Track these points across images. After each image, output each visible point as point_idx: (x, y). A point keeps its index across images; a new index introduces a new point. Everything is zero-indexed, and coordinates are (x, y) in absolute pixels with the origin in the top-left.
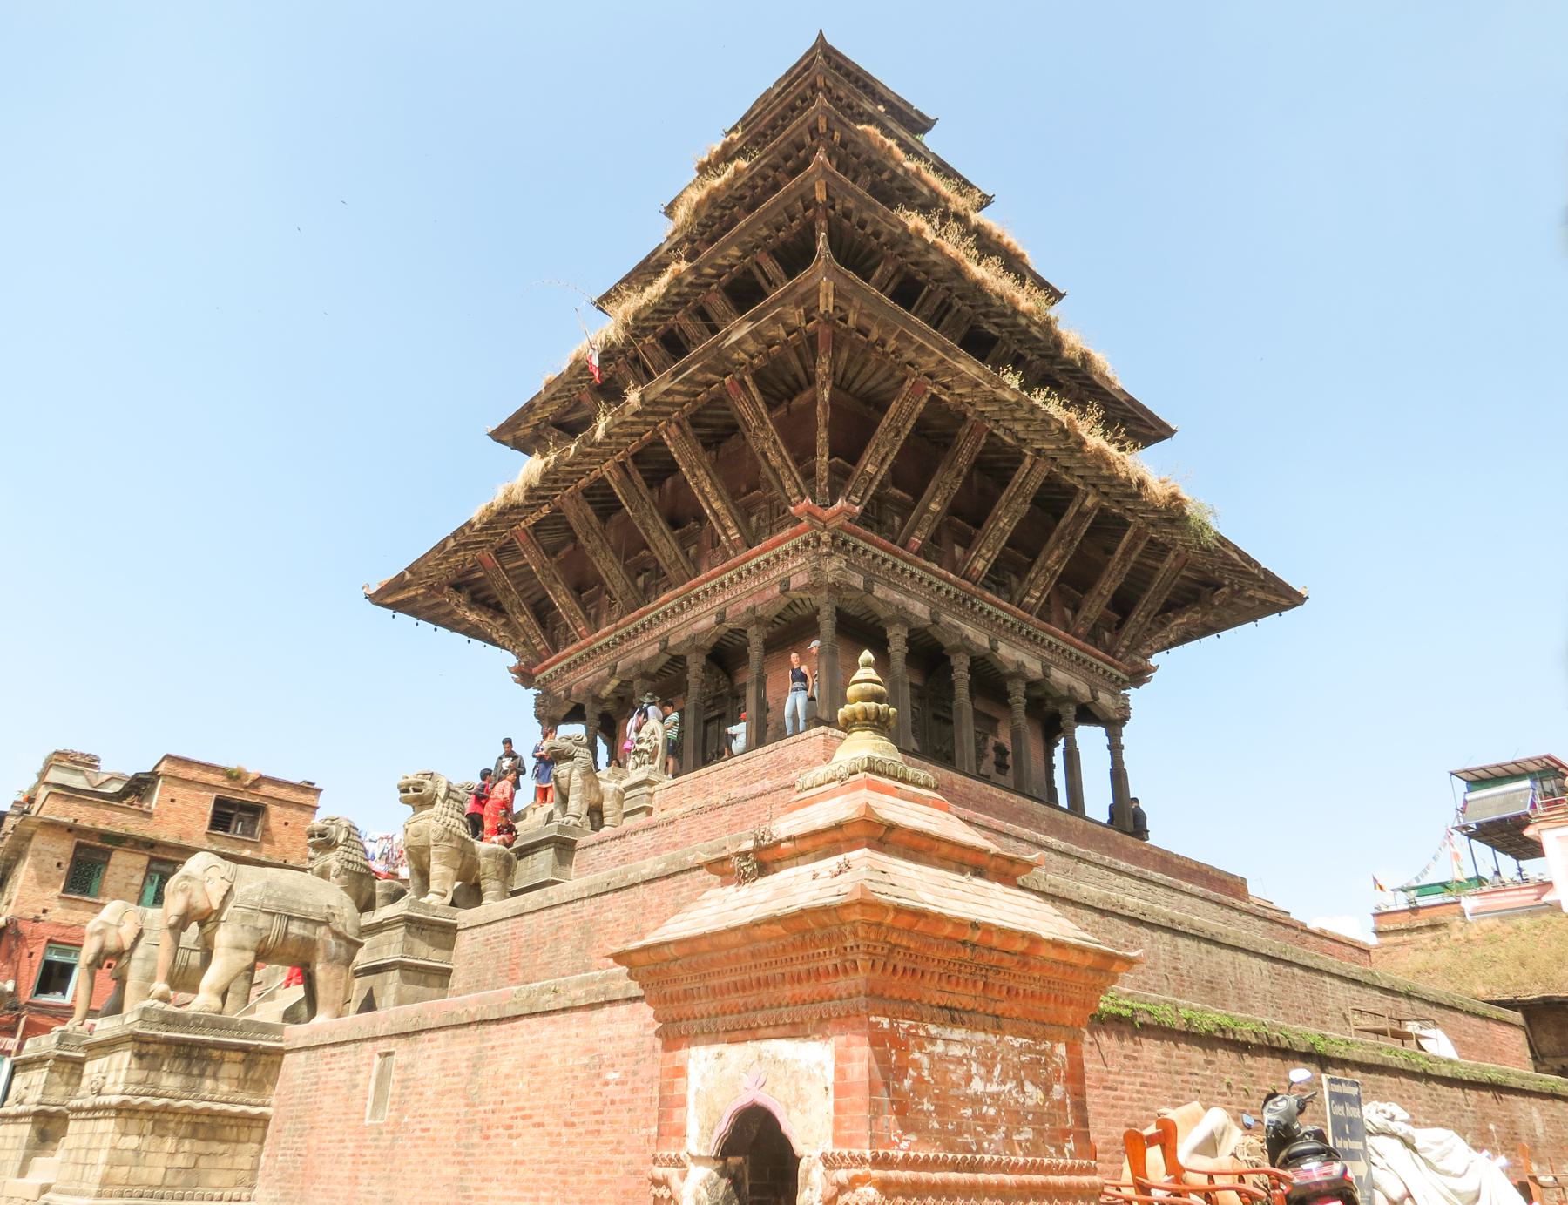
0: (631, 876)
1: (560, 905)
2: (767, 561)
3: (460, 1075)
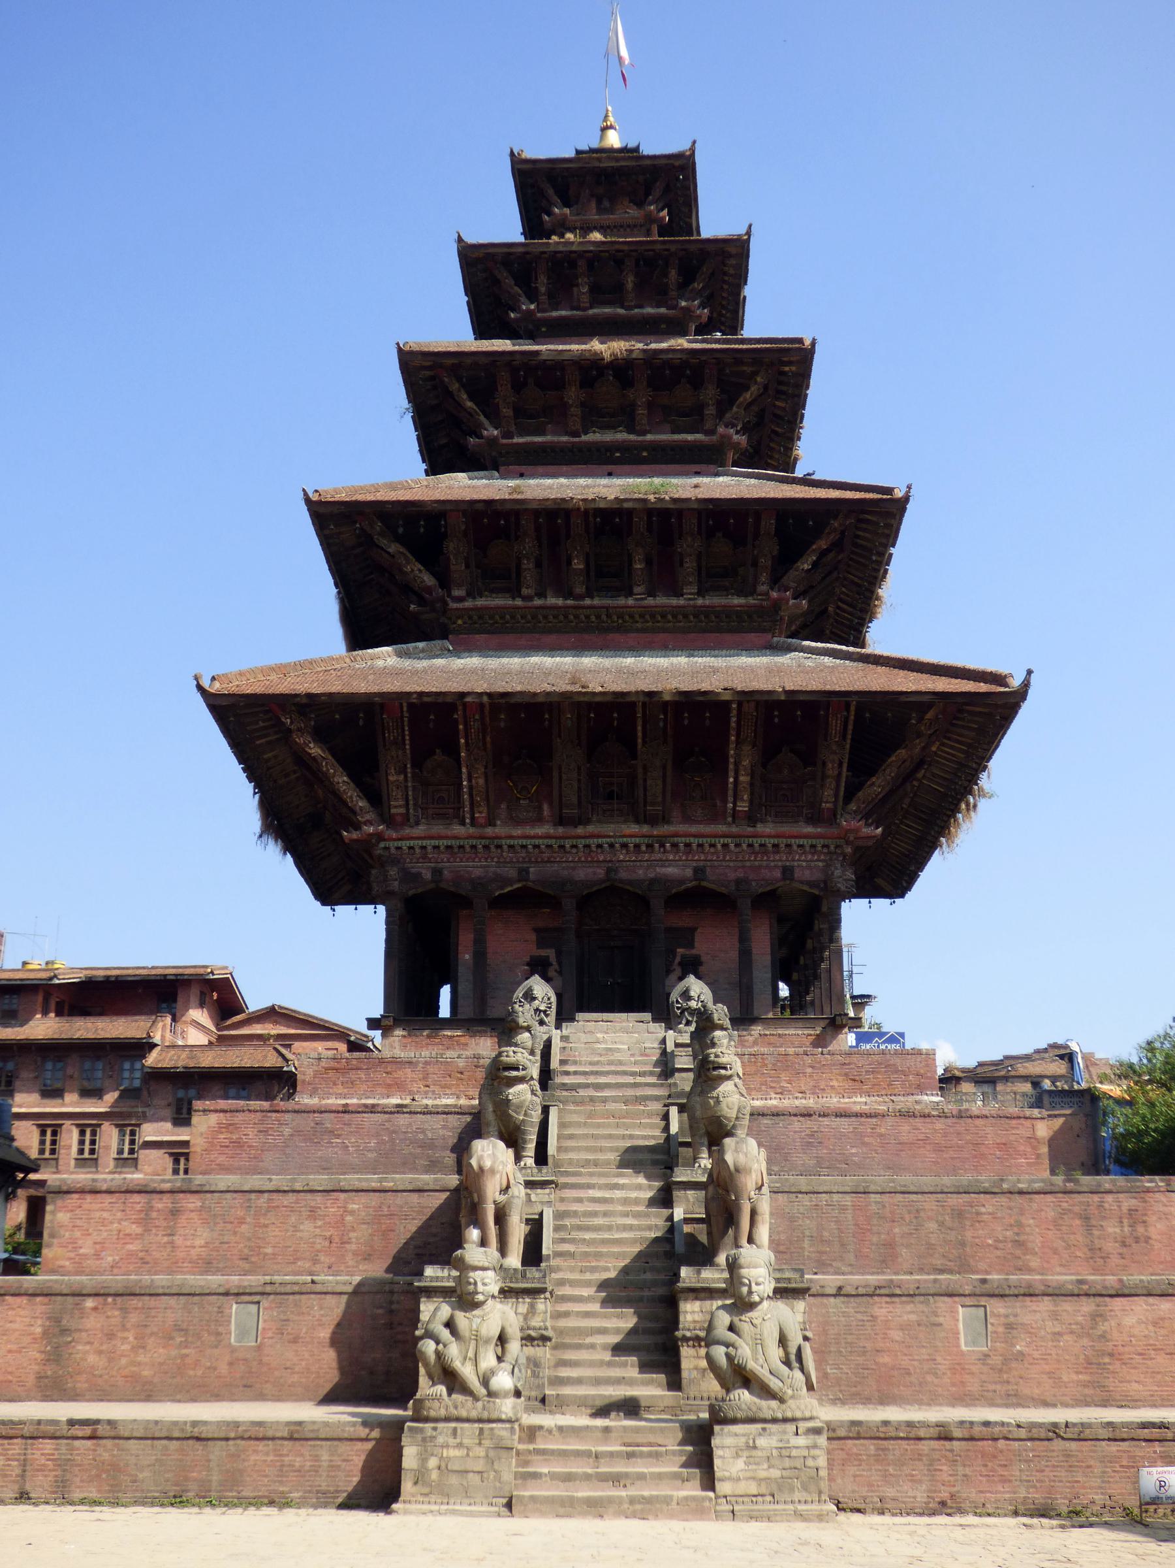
0: (1005, 1186)
1: (916, 1193)
2: (775, 846)
3: (1077, 1324)
